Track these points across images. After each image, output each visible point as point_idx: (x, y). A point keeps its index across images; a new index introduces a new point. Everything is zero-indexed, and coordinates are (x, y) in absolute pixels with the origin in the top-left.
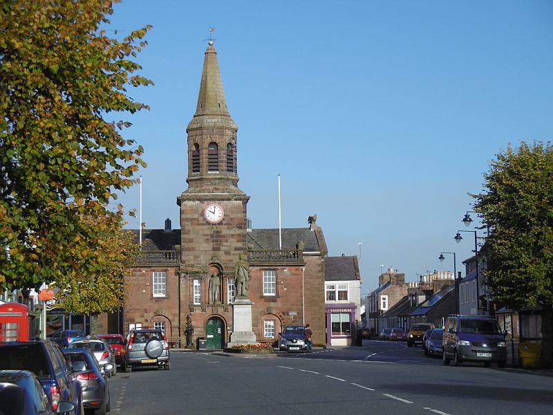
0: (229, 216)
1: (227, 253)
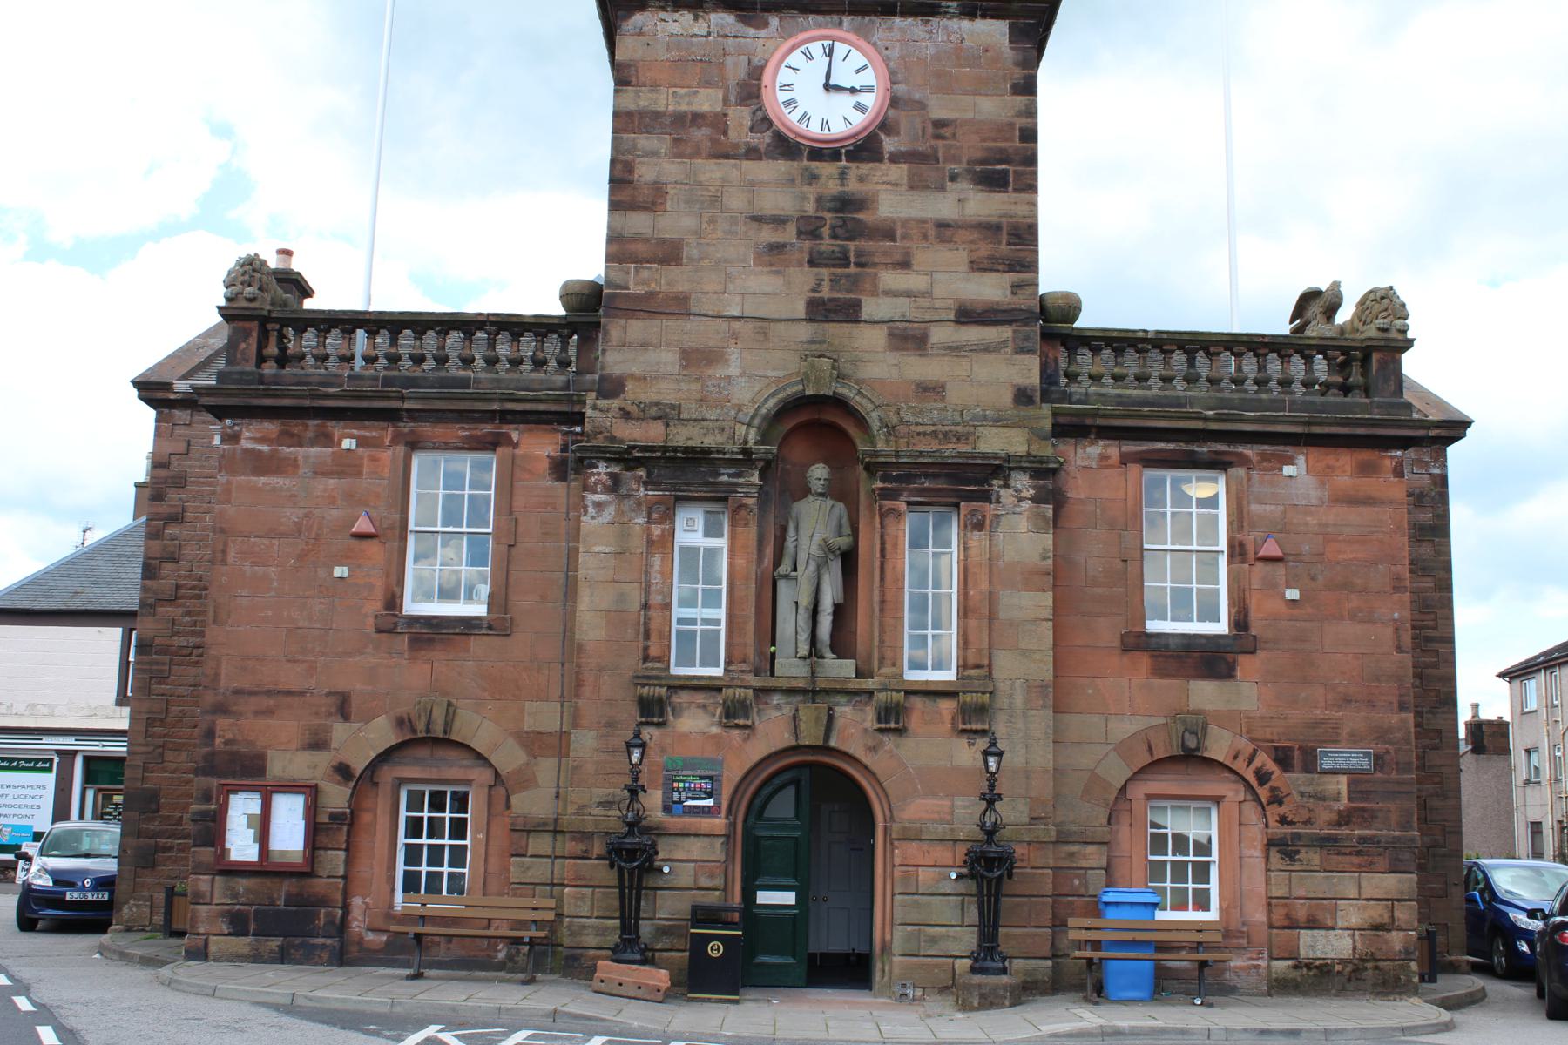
0: (921, 106)
1: (909, 338)
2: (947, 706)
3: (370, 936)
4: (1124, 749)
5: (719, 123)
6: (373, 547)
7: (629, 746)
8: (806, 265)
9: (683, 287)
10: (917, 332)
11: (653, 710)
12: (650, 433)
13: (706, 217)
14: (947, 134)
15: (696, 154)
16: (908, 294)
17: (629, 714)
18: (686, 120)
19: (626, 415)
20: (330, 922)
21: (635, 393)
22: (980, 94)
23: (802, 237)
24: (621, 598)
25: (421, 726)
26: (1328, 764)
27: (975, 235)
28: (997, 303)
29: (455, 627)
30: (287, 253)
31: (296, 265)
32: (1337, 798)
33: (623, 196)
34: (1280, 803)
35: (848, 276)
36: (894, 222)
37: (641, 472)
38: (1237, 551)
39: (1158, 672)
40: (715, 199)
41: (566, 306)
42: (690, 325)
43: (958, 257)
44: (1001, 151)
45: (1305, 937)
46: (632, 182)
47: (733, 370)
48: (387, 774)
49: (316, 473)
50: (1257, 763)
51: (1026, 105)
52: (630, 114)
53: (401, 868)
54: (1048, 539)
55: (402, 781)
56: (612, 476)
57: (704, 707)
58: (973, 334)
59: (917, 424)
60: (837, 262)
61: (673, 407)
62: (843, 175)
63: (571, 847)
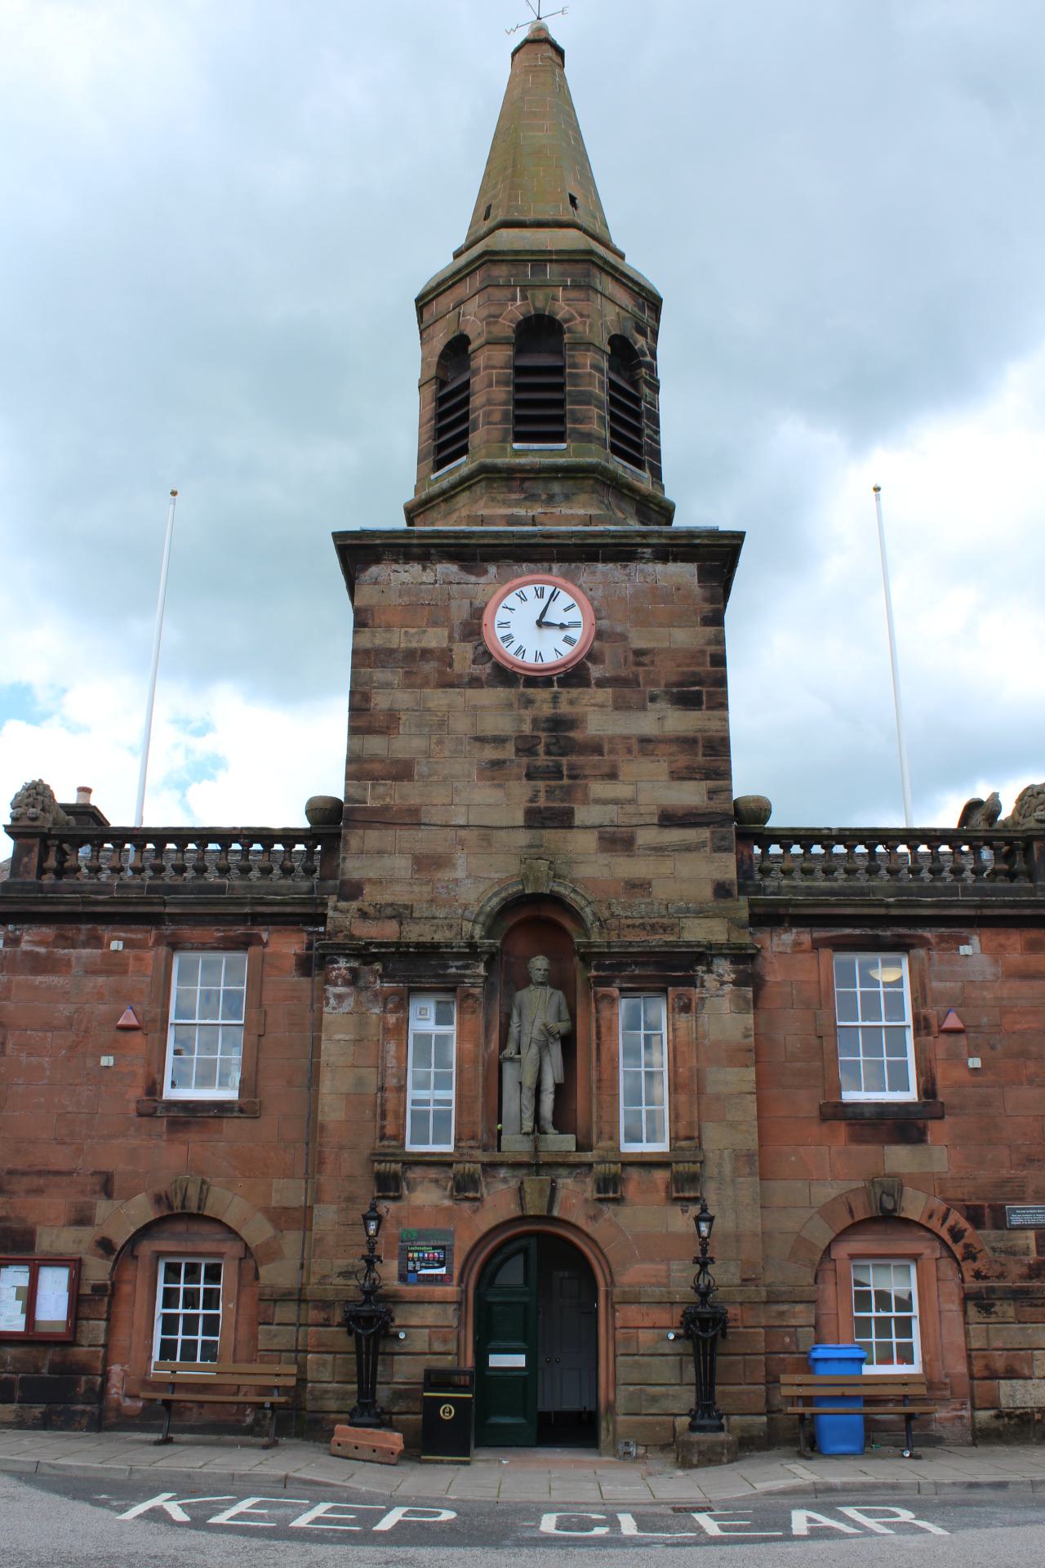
1: (617, 841)
2: (661, 1176)
3: (128, 1402)
4: (826, 1211)
5: (445, 657)
6: (137, 1038)
7: (366, 1219)
8: (524, 779)
9: (414, 800)
10: (625, 835)
11: (389, 1185)
12: (388, 931)
13: (434, 739)
14: (646, 662)
15: (425, 684)
16: (615, 802)
17: (366, 1190)
18: (414, 656)
19: (364, 915)
20: (91, 1388)
21: (372, 896)
22: (674, 627)
23: (520, 754)
24: (360, 1082)
25: (177, 1202)
26: (1016, 1220)
27: (674, 748)
28: (696, 808)
29: (209, 1111)
30: (86, 791)
31: (94, 801)
32: (1026, 1252)
33: (359, 723)
34: (974, 1259)
35: (562, 787)
36: (601, 738)
37: (378, 966)
38: (922, 1025)
39: (856, 1139)
40: (442, 724)
41: (310, 820)
42: (422, 834)
43: (661, 767)
44: (694, 674)
45: (1005, 1386)
46: (369, 710)
47: (460, 873)
48: (146, 1248)
49: (87, 972)
50: (950, 1222)
51: (715, 635)
52: (367, 652)
53: (158, 1336)
54: (749, 1019)
55: (159, 1255)
56: (351, 970)
57: (436, 1181)
58: (675, 835)
59: (626, 917)
60: (551, 775)
61: (406, 907)
62: (555, 699)
63: (314, 1315)
